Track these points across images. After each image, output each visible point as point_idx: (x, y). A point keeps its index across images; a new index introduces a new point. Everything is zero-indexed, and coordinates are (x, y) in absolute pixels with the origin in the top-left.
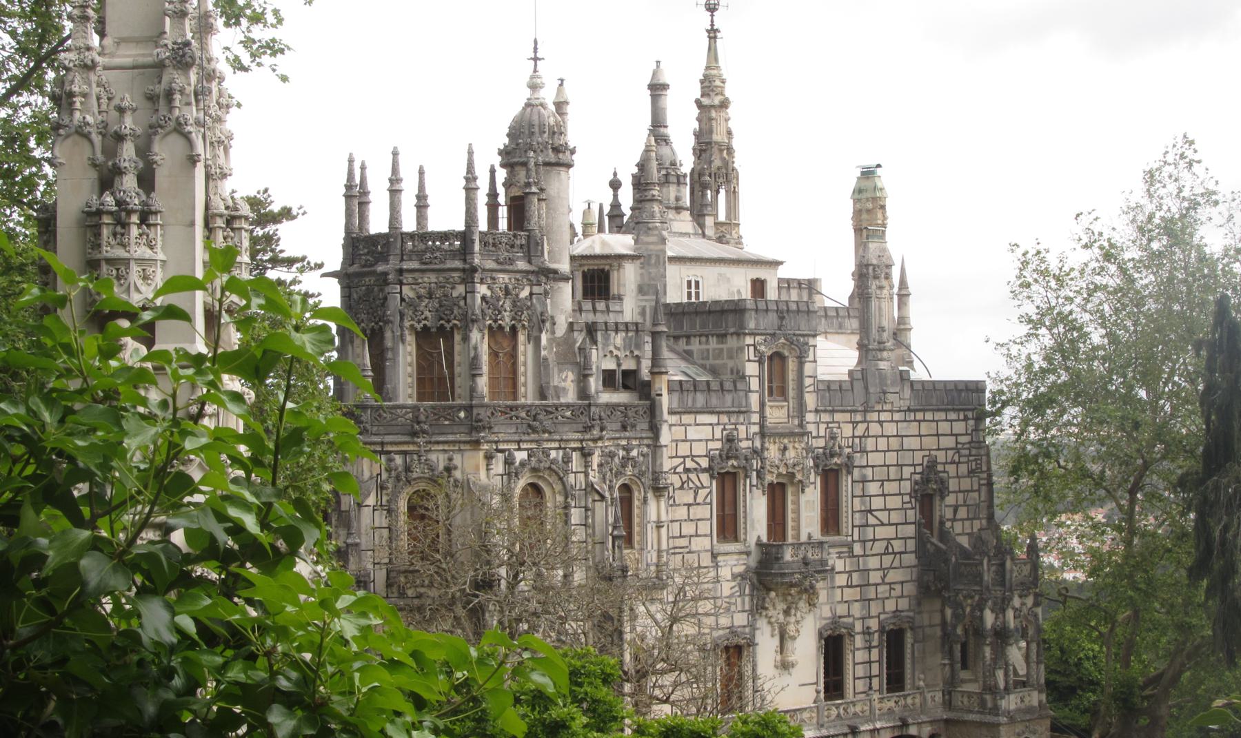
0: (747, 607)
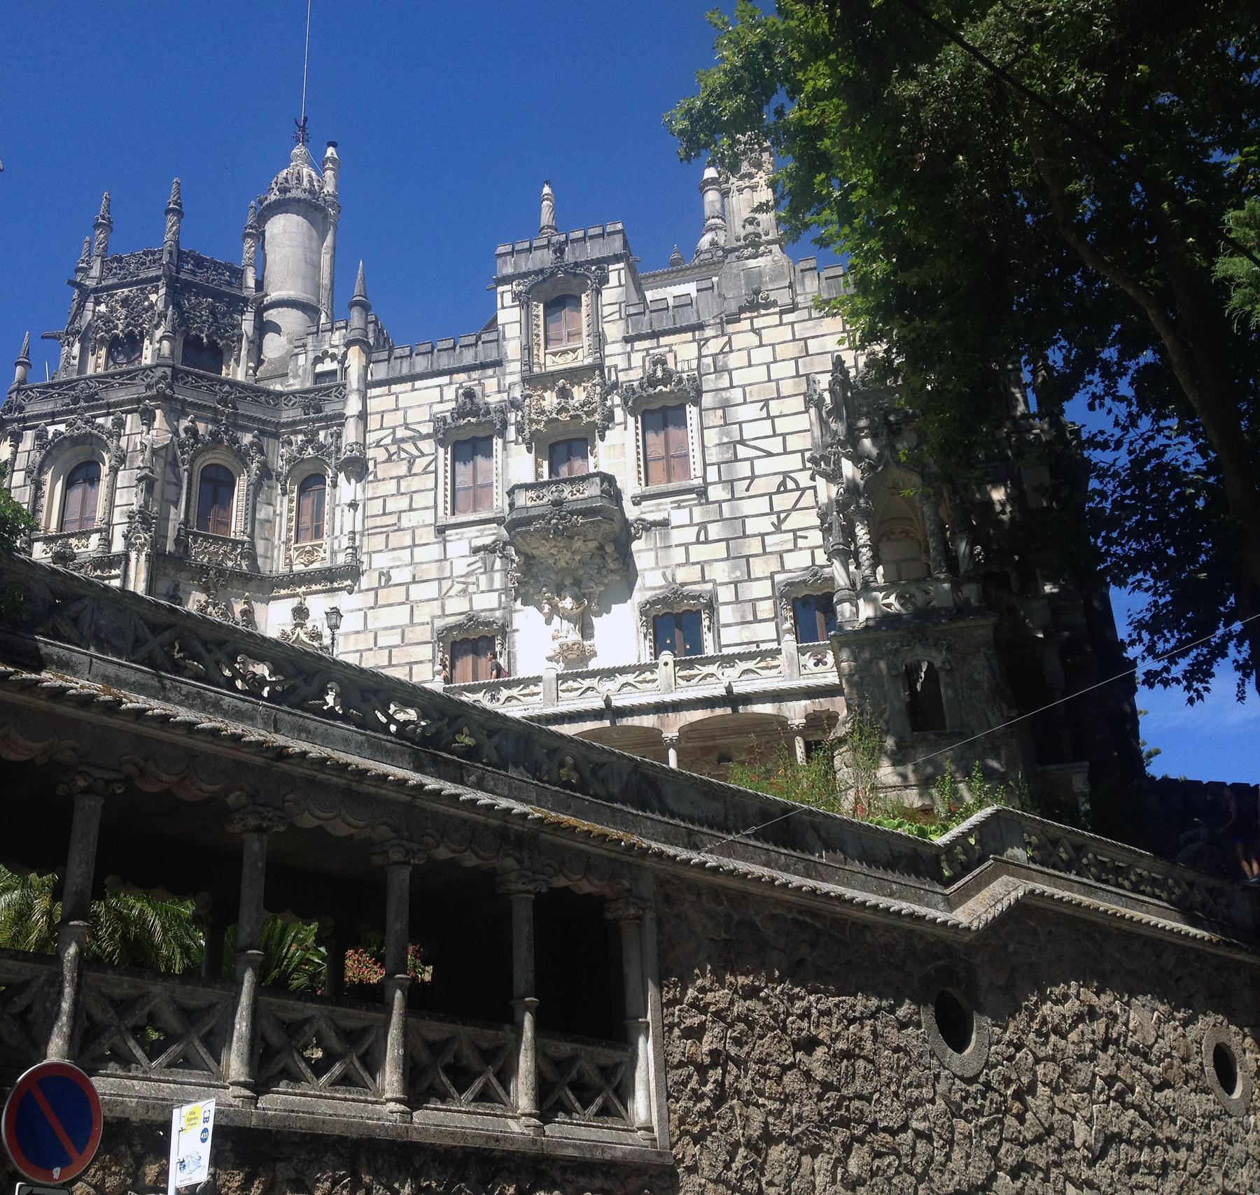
0: (498, 584)
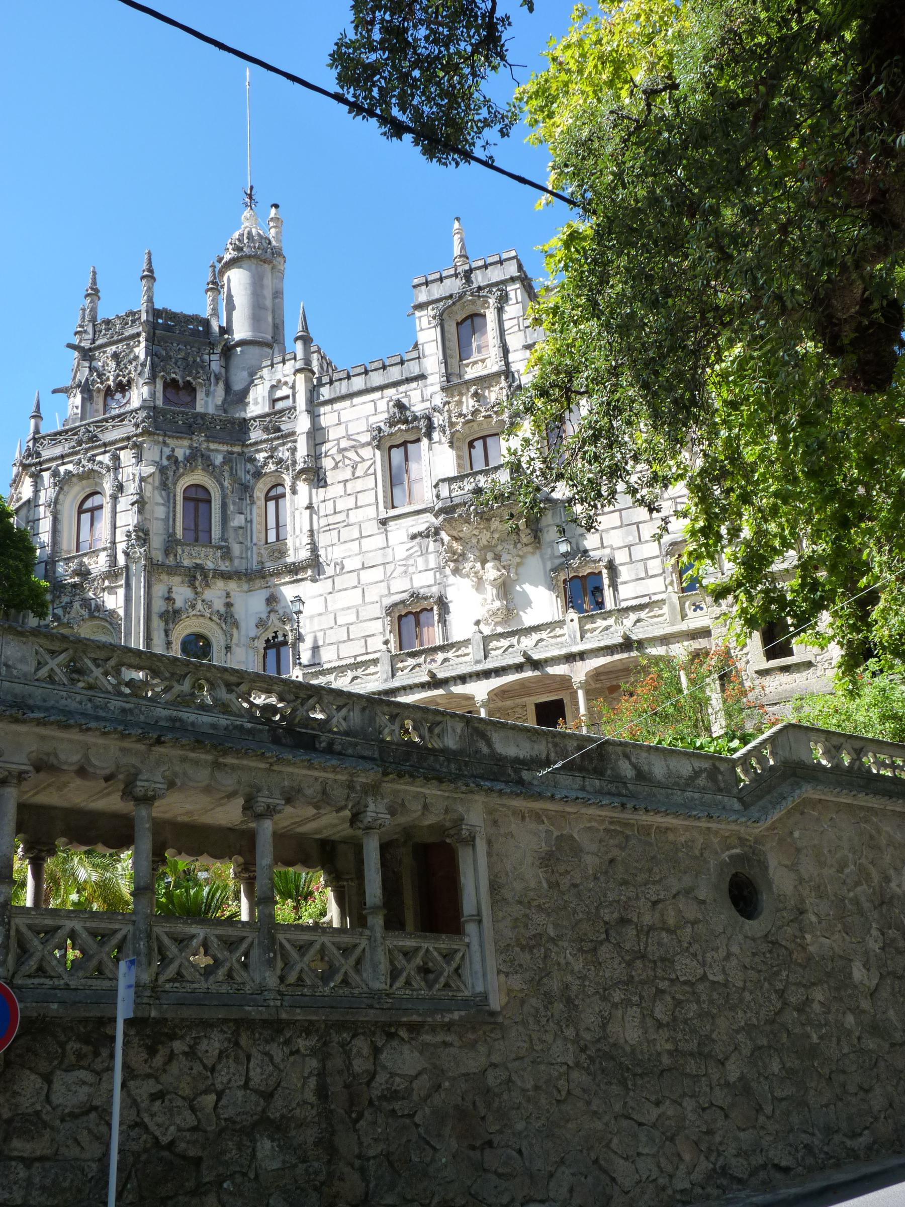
0: (432, 564)
